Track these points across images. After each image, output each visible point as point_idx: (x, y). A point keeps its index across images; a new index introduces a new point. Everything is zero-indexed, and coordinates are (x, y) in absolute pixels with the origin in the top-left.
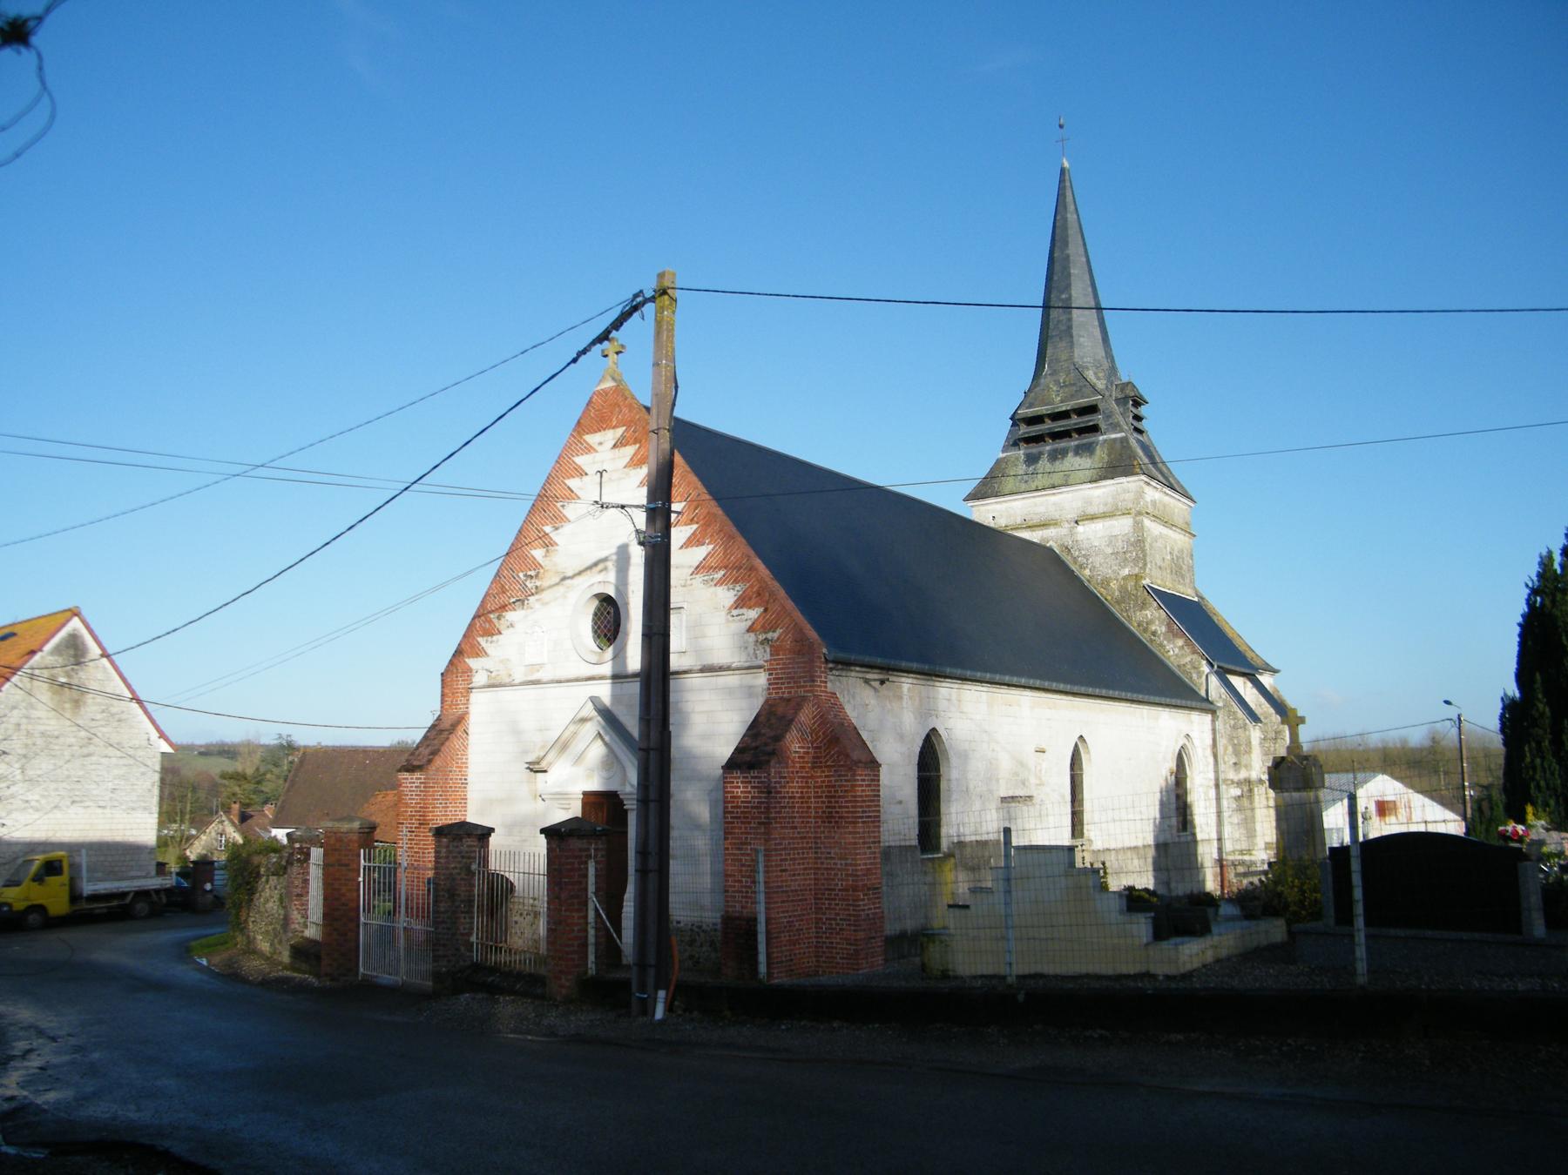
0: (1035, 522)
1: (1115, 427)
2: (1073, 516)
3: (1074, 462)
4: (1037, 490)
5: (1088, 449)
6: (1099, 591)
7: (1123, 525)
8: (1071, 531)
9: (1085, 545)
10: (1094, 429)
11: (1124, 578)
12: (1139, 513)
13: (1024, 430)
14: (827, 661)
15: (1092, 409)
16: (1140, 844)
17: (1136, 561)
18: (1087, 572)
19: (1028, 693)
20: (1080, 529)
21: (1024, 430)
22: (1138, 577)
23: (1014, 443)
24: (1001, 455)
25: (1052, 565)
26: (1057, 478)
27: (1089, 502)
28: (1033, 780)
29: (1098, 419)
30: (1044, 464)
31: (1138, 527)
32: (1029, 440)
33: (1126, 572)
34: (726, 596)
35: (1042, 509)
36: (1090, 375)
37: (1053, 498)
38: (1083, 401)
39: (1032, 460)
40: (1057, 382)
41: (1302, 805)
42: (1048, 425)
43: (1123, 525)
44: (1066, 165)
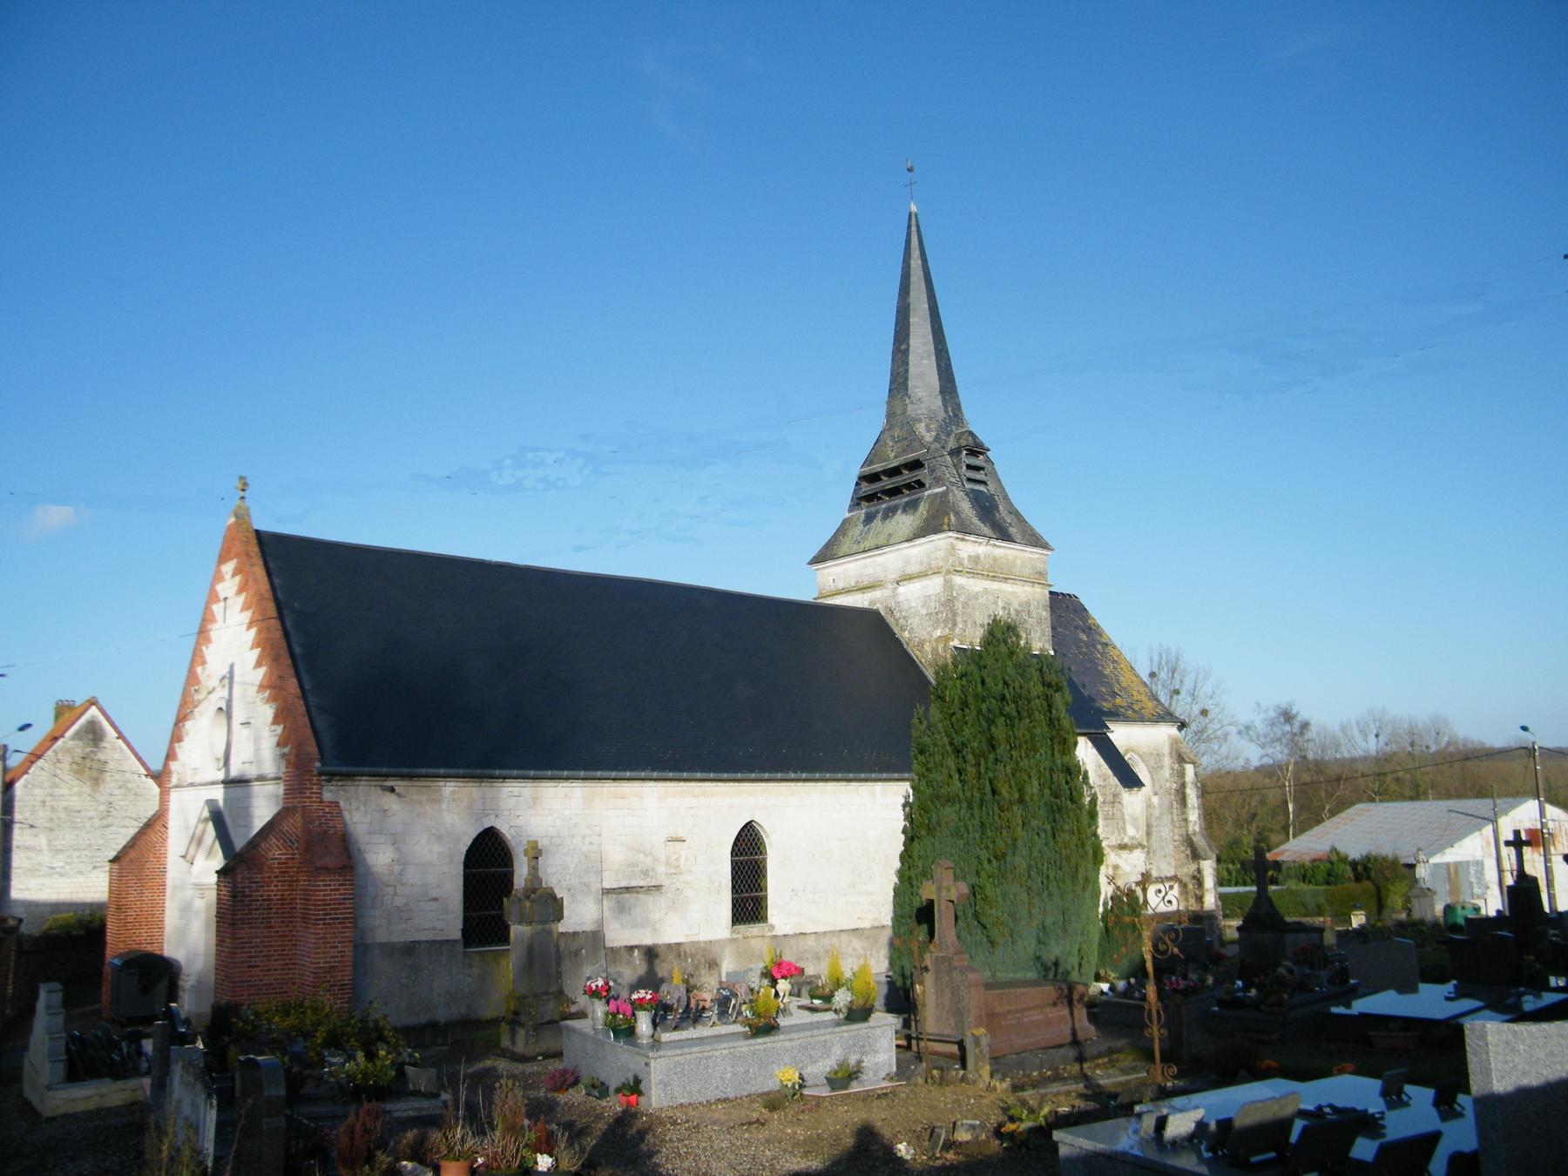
0: (866, 583)
1: (938, 481)
2: (895, 576)
3: (904, 522)
4: (864, 551)
5: (912, 506)
6: (915, 653)
7: (934, 585)
8: (894, 595)
9: (904, 606)
10: (921, 485)
11: (937, 640)
12: (948, 572)
13: (867, 488)
14: (320, 774)
15: (916, 465)
16: (866, 924)
17: (946, 621)
18: (906, 634)
19: (652, 784)
20: (901, 589)
21: (867, 488)
22: (946, 639)
23: (859, 500)
24: (848, 515)
25: (873, 628)
26: (881, 541)
27: (907, 562)
28: (661, 869)
29: (923, 474)
30: (877, 522)
31: (948, 586)
32: (870, 498)
33: (938, 633)
34: (268, 712)
35: (871, 571)
36: (921, 428)
37: (879, 559)
38: (911, 456)
39: (869, 519)
40: (893, 437)
41: (544, 930)
42: (887, 483)
43: (934, 585)
44: (914, 208)
